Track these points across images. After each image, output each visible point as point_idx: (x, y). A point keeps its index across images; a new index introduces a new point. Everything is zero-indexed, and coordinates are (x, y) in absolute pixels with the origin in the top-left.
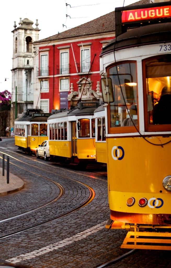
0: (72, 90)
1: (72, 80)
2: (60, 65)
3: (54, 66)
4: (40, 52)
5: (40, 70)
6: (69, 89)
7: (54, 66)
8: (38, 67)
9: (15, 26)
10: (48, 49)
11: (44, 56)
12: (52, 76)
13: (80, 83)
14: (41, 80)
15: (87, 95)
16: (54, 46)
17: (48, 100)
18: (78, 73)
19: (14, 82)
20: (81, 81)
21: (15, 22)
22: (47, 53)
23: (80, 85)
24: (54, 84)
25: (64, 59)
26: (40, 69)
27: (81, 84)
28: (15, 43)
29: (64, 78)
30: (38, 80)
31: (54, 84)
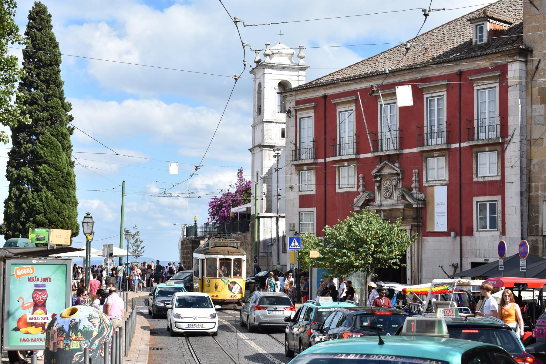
0: (361, 189)
1: (363, 167)
2: (338, 136)
3: (326, 140)
4: (296, 111)
5: (298, 148)
6: (356, 186)
7: (326, 140)
8: (294, 142)
10: (312, 105)
11: (306, 119)
12: (322, 160)
13: (378, 174)
14: (299, 168)
15: (392, 199)
16: (325, 97)
17: (314, 209)
18: (374, 152)
19: (256, 174)
20: (380, 170)
22: (312, 113)
23: (378, 179)
24: (326, 176)
26: (298, 145)
27: (380, 176)
28: (256, 95)
31: (326, 176)
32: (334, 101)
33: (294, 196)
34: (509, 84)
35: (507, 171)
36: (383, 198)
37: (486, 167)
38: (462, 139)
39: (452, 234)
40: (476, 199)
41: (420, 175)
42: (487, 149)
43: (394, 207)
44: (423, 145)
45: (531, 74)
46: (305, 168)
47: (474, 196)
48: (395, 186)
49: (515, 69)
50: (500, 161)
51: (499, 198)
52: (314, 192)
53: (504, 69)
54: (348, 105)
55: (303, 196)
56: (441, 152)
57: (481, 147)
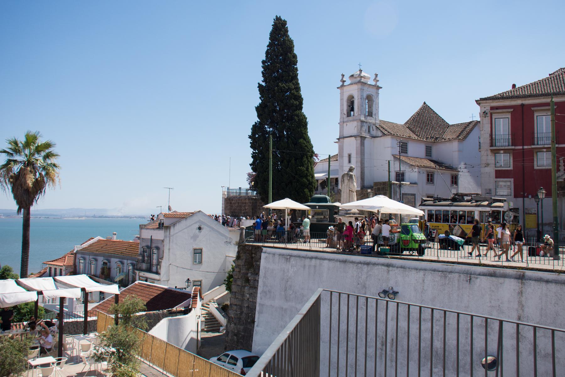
4: (491, 114)
10: (512, 110)
14: (495, 152)
16: (523, 105)
22: (509, 116)
26: (494, 136)
29: (545, 150)
30: (489, 152)
32: (533, 109)
33: (491, 170)
46: (502, 152)
52: (511, 168)
55: (499, 170)
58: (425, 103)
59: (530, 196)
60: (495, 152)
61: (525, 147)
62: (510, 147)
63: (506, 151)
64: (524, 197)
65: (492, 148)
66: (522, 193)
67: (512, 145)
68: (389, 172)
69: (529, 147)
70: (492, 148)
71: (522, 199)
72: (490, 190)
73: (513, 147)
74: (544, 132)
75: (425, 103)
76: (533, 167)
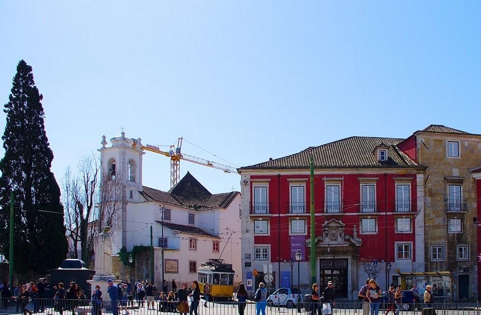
4: (251, 183)
6: (306, 232)
9: (104, 142)
14: (255, 219)
16: (279, 176)
21: (104, 137)
22: (267, 185)
25: (297, 194)
26: (253, 204)
29: (298, 218)
32: (288, 180)
34: (417, 185)
35: (417, 229)
36: (330, 240)
37: (403, 226)
38: (387, 210)
39: (383, 261)
40: (396, 243)
41: (358, 227)
42: (404, 217)
43: (338, 246)
44: (395, 211)
45: (425, 181)
46: (261, 219)
47: (396, 241)
48: (340, 234)
49: (420, 178)
50: (412, 224)
51: (412, 243)
53: (415, 176)
54: (300, 183)
56: (373, 216)
57: (401, 216)
58: (188, 172)
59: (285, 261)
60: (255, 219)
61: (281, 215)
62: (268, 215)
63: (264, 218)
64: (279, 261)
65: (251, 215)
66: (278, 258)
67: (270, 213)
68: (152, 237)
69: (285, 215)
70: (251, 215)
71: (278, 263)
72: (250, 255)
73: (271, 215)
74: (298, 201)
75: (188, 172)
76: (288, 233)
